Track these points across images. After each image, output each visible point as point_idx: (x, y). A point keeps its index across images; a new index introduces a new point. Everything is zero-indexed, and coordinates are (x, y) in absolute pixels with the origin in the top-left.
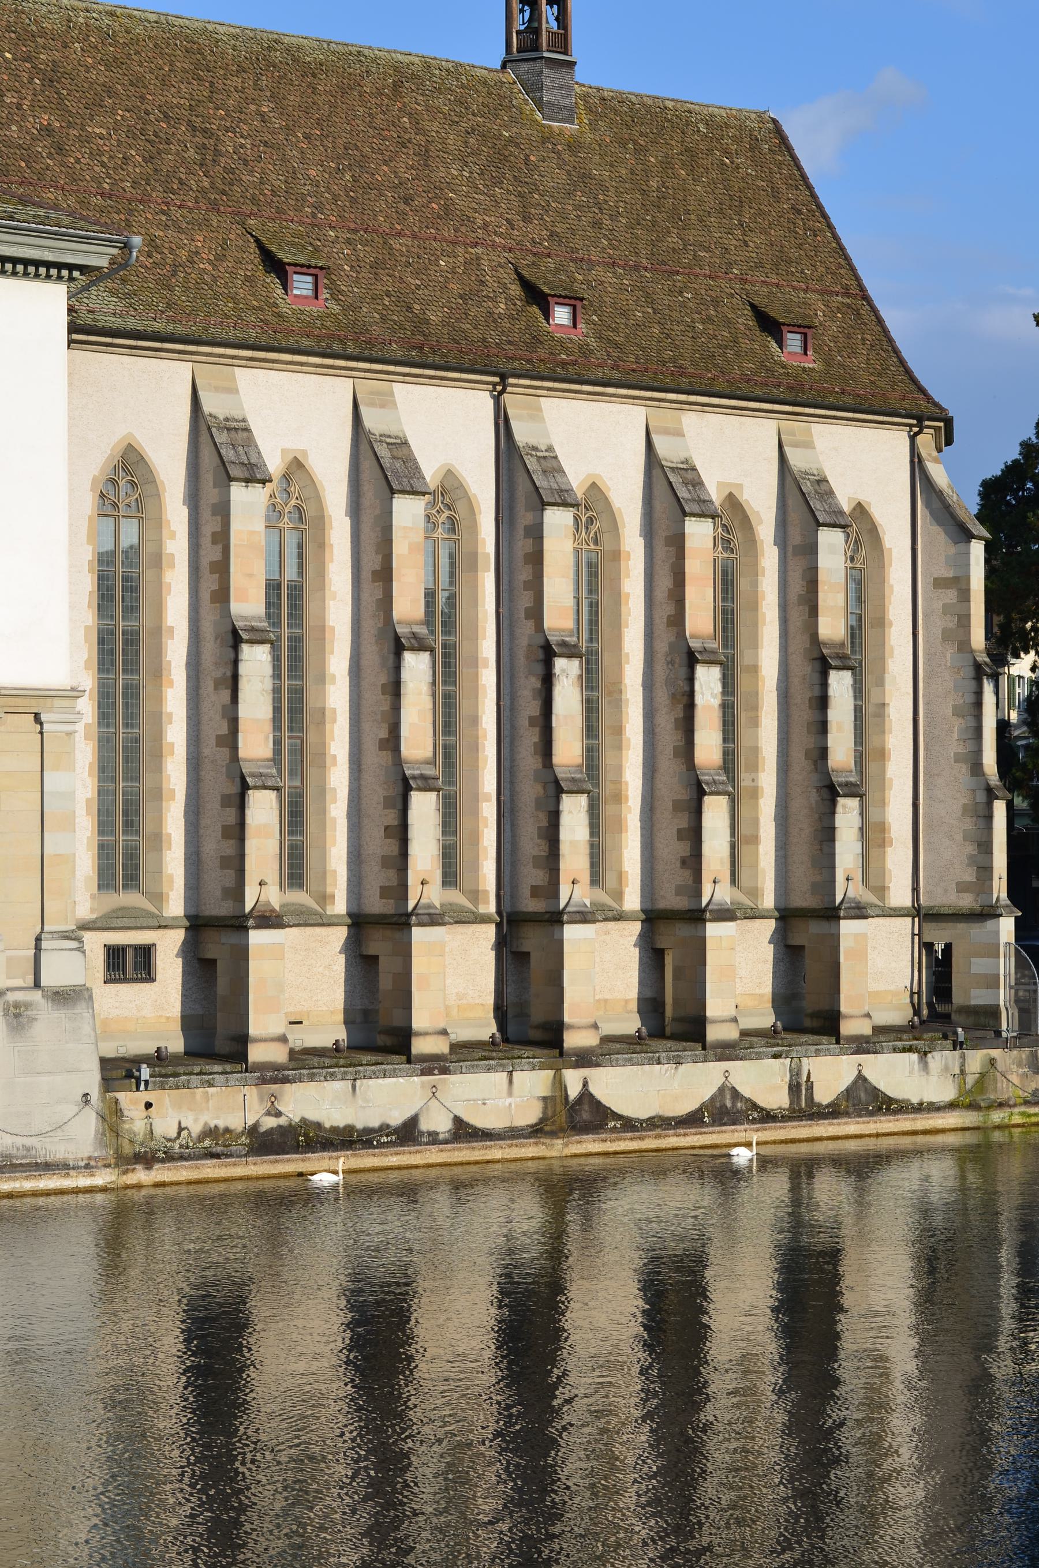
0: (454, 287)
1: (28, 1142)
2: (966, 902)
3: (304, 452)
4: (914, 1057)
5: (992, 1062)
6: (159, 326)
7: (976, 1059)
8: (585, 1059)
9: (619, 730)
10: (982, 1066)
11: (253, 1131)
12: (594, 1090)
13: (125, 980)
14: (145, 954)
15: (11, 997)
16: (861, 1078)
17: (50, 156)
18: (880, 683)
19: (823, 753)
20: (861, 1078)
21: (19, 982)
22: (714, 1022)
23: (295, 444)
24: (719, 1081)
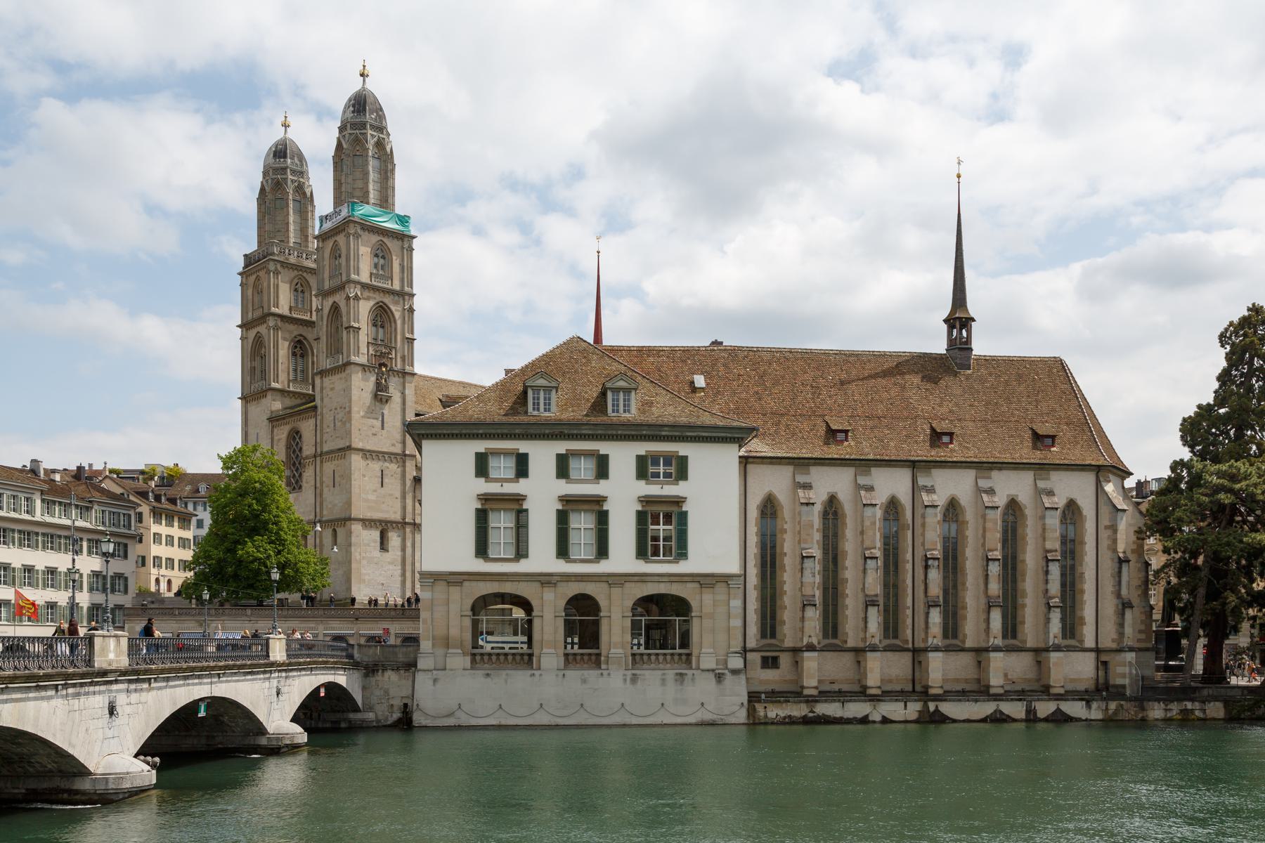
0: (904, 433)
1: (722, 717)
2: (1114, 646)
3: (836, 493)
4: (1084, 703)
5: (1122, 706)
6: (779, 455)
7: (1113, 706)
8: (937, 698)
9: (964, 584)
10: (1117, 707)
11: (805, 716)
12: (940, 709)
13: (769, 668)
14: (775, 659)
15: (717, 671)
16: (1058, 710)
17: (755, 401)
18: (1081, 565)
19: (1047, 591)
20: (1058, 710)
21: (721, 667)
22: (994, 687)
23: (832, 490)
24: (995, 708)
